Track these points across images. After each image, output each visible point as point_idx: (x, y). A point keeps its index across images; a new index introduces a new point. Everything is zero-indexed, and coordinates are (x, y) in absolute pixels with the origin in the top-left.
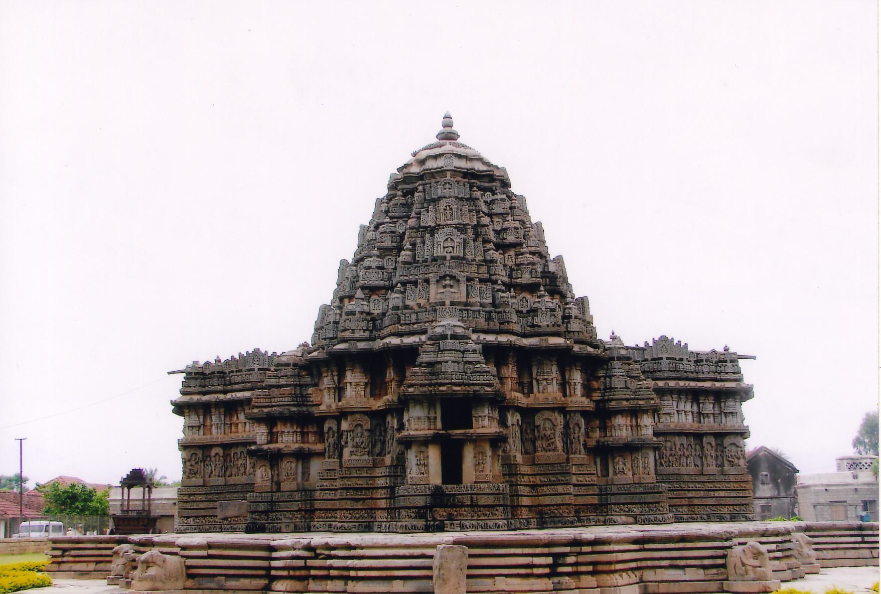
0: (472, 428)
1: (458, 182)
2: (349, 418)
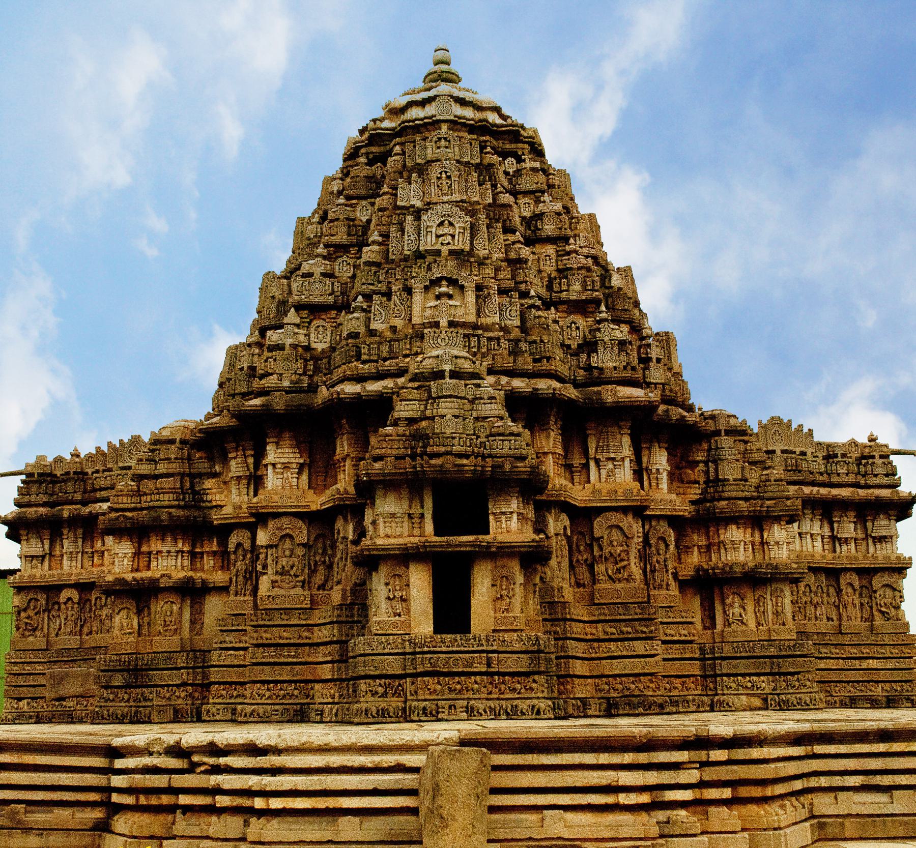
2: (271, 524)
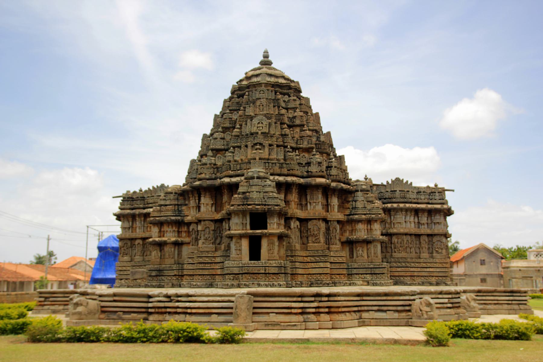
0: (266, 228)
1: (268, 90)
2: (202, 223)
